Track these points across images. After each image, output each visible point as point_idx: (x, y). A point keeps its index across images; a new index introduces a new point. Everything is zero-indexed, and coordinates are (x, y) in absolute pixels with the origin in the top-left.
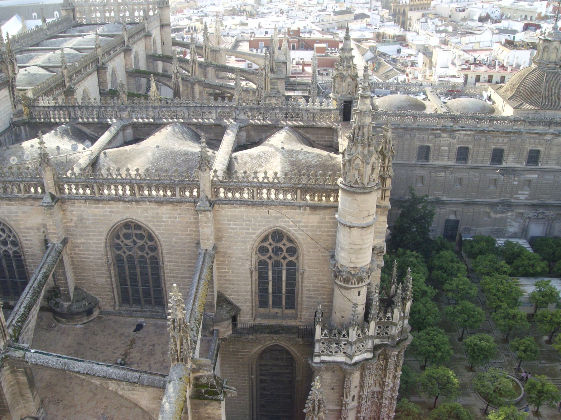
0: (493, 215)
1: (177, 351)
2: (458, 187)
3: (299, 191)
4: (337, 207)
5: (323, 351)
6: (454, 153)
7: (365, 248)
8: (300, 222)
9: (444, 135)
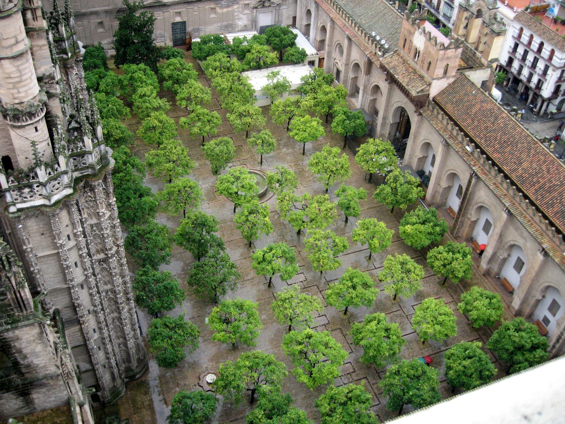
0: (219, 10)
5: (16, 199)
7: (25, 80)
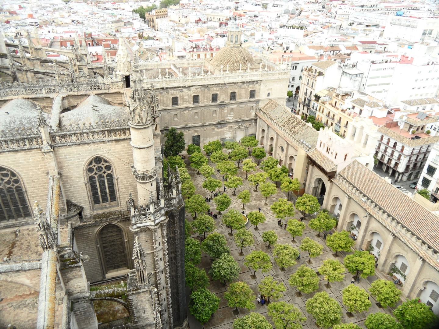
1: (45, 242)
2: (196, 117)
3: (106, 132)
4: (130, 139)
6: (192, 99)
8: (110, 150)
9: (184, 90)
